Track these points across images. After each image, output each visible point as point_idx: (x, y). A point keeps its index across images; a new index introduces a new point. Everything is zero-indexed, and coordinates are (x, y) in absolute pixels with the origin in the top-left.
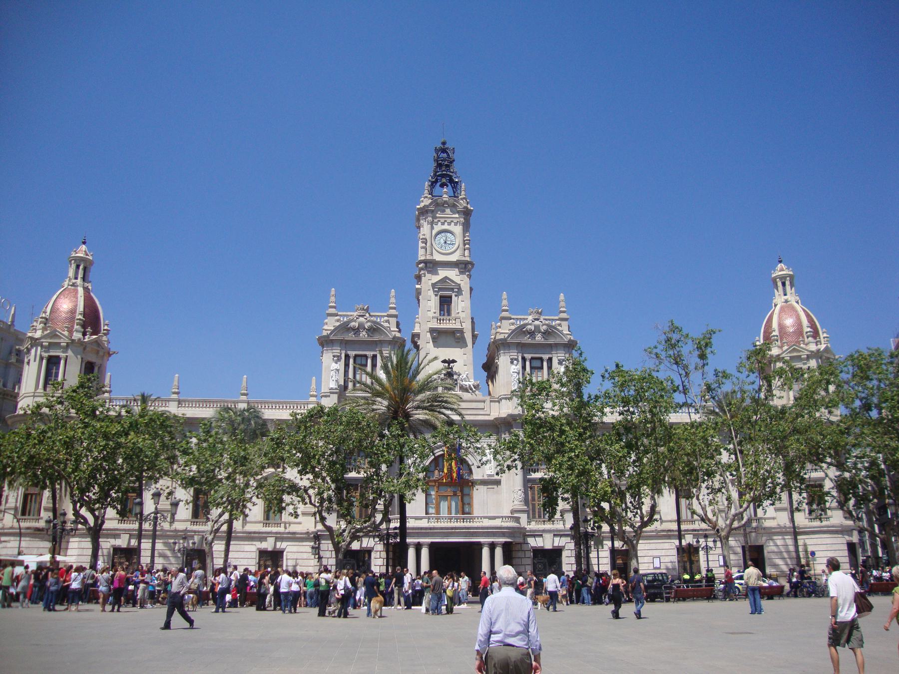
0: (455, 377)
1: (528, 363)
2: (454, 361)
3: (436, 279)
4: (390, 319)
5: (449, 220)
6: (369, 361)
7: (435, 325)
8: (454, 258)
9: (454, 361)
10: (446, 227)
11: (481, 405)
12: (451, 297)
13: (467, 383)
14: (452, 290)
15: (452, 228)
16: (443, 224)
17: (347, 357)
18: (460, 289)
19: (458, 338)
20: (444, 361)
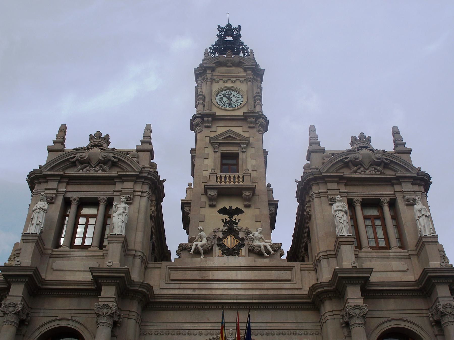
0: (241, 235)
1: (358, 208)
2: (238, 211)
3: (213, 135)
4: (141, 154)
5: (233, 79)
6: (102, 207)
7: (213, 182)
8: (240, 113)
9: (238, 211)
10: (229, 84)
11: (285, 275)
12: (235, 156)
13: (262, 244)
14: (238, 145)
15: (238, 85)
16: (226, 82)
17: (67, 203)
18: (248, 144)
19: (248, 199)
20: (223, 211)
